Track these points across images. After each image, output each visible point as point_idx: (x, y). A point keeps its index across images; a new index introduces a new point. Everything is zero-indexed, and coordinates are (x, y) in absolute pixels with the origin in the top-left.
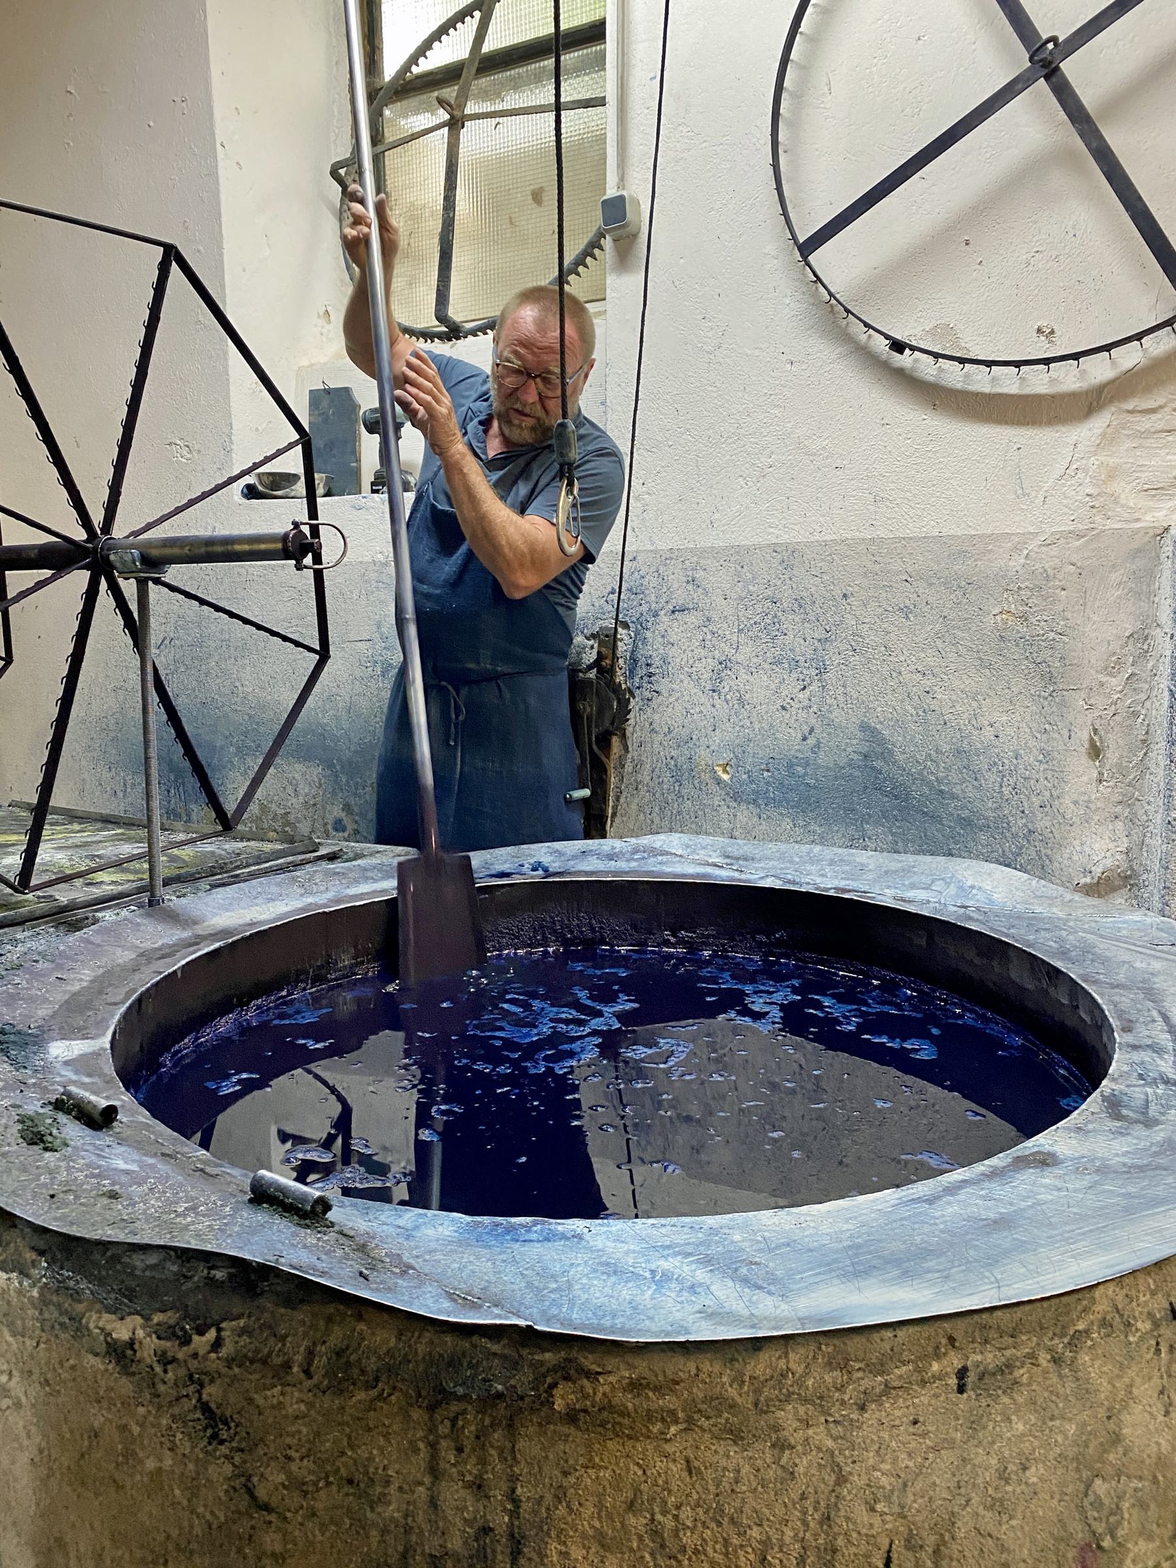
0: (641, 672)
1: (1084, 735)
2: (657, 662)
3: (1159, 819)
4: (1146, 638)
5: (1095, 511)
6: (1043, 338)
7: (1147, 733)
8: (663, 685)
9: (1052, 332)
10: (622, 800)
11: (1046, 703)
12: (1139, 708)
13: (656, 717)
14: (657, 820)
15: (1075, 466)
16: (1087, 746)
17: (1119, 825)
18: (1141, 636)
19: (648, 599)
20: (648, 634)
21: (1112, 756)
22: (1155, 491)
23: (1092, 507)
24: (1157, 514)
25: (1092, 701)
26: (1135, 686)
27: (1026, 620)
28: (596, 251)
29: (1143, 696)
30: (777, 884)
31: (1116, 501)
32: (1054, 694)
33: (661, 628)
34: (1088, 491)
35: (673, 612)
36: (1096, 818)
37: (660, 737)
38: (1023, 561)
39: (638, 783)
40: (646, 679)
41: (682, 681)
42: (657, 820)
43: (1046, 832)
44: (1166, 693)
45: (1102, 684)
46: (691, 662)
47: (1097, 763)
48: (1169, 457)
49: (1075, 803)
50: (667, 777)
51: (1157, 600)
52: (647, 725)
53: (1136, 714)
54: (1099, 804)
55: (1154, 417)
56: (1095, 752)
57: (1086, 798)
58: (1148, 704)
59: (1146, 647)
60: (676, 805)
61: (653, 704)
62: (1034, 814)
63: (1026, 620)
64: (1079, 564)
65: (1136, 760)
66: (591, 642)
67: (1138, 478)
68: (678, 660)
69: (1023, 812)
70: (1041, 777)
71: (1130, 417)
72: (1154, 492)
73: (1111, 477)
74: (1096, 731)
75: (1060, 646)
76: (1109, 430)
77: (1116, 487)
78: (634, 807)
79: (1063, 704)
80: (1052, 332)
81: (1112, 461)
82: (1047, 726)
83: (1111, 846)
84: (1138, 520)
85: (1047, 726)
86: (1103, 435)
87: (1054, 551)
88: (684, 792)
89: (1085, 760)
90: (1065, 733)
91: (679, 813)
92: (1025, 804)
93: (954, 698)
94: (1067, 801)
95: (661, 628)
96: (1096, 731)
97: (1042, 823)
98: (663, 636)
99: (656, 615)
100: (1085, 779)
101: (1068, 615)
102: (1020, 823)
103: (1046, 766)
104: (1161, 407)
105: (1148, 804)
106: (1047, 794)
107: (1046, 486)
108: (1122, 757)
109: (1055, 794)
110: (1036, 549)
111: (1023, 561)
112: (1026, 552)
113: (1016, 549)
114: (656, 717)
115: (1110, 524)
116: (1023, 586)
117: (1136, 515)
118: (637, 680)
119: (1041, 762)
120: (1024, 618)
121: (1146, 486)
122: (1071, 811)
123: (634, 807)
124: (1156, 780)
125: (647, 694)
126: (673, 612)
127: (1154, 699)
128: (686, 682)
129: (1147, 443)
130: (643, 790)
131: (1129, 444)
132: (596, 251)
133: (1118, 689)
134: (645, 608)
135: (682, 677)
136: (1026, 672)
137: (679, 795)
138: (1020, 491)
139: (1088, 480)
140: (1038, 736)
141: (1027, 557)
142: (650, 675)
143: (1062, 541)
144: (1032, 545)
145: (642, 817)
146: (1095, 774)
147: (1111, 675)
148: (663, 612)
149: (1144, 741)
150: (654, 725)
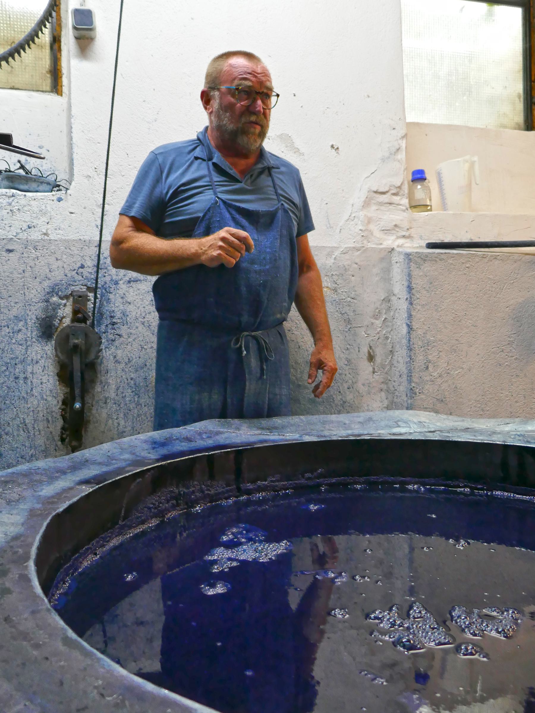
0: (106, 321)
1: (365, 350)
2: (118, 315)
3: (402, 388)
4: (389, 301)
5: (363, 238)
6: (334, 150)
7: (392, 347)
8: (123, 330)
9: (338, 148)
10: (94, 411)
11: (347, 335)
12: (388, 335)
13: (119, 352)
14: (122, 423)
15: (353, 215)
16: (367, 355)
17: (383, 394)
18: (387, 300)
19: (110, 273)
20: (111, 296)
21: (378, 360)
22: (386, 231)
23: (363, 236)
24: (390, 242)
25: (369, 332)
26: (386, 324)
27: (336, 291)
28: (10, 59)
29: (389, 329)
30: (315, 439)
31: (372, 234)
32: (351, 330)
33: (121, 292)
34: (361, 228)
35: (129, 282)
36: (373, 391)
37: (122, 365)
38: (333, 261)
39: (106, 399)
40: (110, 326)
41: (137, 328)
42: (122, 423)
43: (351, 402)
44: (404, 325)
45: (372, 324)
46: (143, 315)
47: (372, 364)
48: (391, 216)
49: (363, 385)
50: (128, 393)
51: (392, 283)
52: (111, 357)
53: (387, 338)
54: (374, 384)
55: (384, 196)
56: (371, 358)
57: (368, 382)
58: (392, 333)
59: (389, 305)
60: (136, 411)
61: (117, 343)
62: (345, 393)
63: (336, 291)
64: (359, 264)
65: (388, 361)
66: (64, 301)
67: (379, 224)
68: (134, 314)
69: (340, 392)
70: (347, 373)
71: (375, 195)
72: (386, 232)
73: (369, 222)
74: (370, 347)
75: (353, 305)
76: (367, 200)
77: (371, 227)
78: (104, 415)
79: (355, 335)
80: (338, 148)
81: (369, 215)
82: (348, 346)
83: (380, 404)
84: (381, 244)
85: (348, 346)
86: (365, 202)
87: (347, 256)
88: (142, 401)
89: (366, 363)
90: (357, 349)
91: (139, 416)
92: (341, 388)
93: (303, 333)
94: (360, 385)
95: (121, 292)
96: (370, 347)
97: (349, 397)
98: (122, 298)
99: (116, 283)
100: (367, 372)
101: (356, 289)
102: (339, 398)
103: (349, 367)
104: (387, 192)
105: (394, 382)
106: (350, 381)
107: (341, 224)
108: (382, 360)
109: (354, 381)
110: (339, 255)
111: (333, 261)
112: (334, 256)
113: (329, 255)
114: (119, 352)
115: (370, 245)
116: (334, 274)
117: (381, 242)
118: (103, 328)
119: (346, 365)
120: (335, 290)
121: (383, 229)
122: (363, 389)
123: (104, 415)
124: (398, 370)
125: (111, 337)
126: (129, 282)
127: (394, 330)
128: (140, 328)
129: (382, 208)
130: (110, 404)
131: (374, 207)
132: (10, 59)
133: (380, 325)
134: (108, 279)
135: (137, 324)
136: (337, 318)
137: (138, 404)
138: (328, 226)
139: (360, 222)
140: (344, 351)
141: (335, 259)
142: (114, 324)
143: (350, 252)
144: (337, 253)
145: (110, 421)
146: (371, 369)
147: (376, 319)
148: (121, 282)
149: (391, 351)
150: (118, 358)
